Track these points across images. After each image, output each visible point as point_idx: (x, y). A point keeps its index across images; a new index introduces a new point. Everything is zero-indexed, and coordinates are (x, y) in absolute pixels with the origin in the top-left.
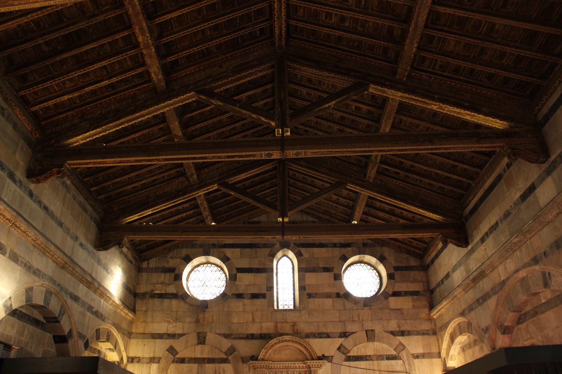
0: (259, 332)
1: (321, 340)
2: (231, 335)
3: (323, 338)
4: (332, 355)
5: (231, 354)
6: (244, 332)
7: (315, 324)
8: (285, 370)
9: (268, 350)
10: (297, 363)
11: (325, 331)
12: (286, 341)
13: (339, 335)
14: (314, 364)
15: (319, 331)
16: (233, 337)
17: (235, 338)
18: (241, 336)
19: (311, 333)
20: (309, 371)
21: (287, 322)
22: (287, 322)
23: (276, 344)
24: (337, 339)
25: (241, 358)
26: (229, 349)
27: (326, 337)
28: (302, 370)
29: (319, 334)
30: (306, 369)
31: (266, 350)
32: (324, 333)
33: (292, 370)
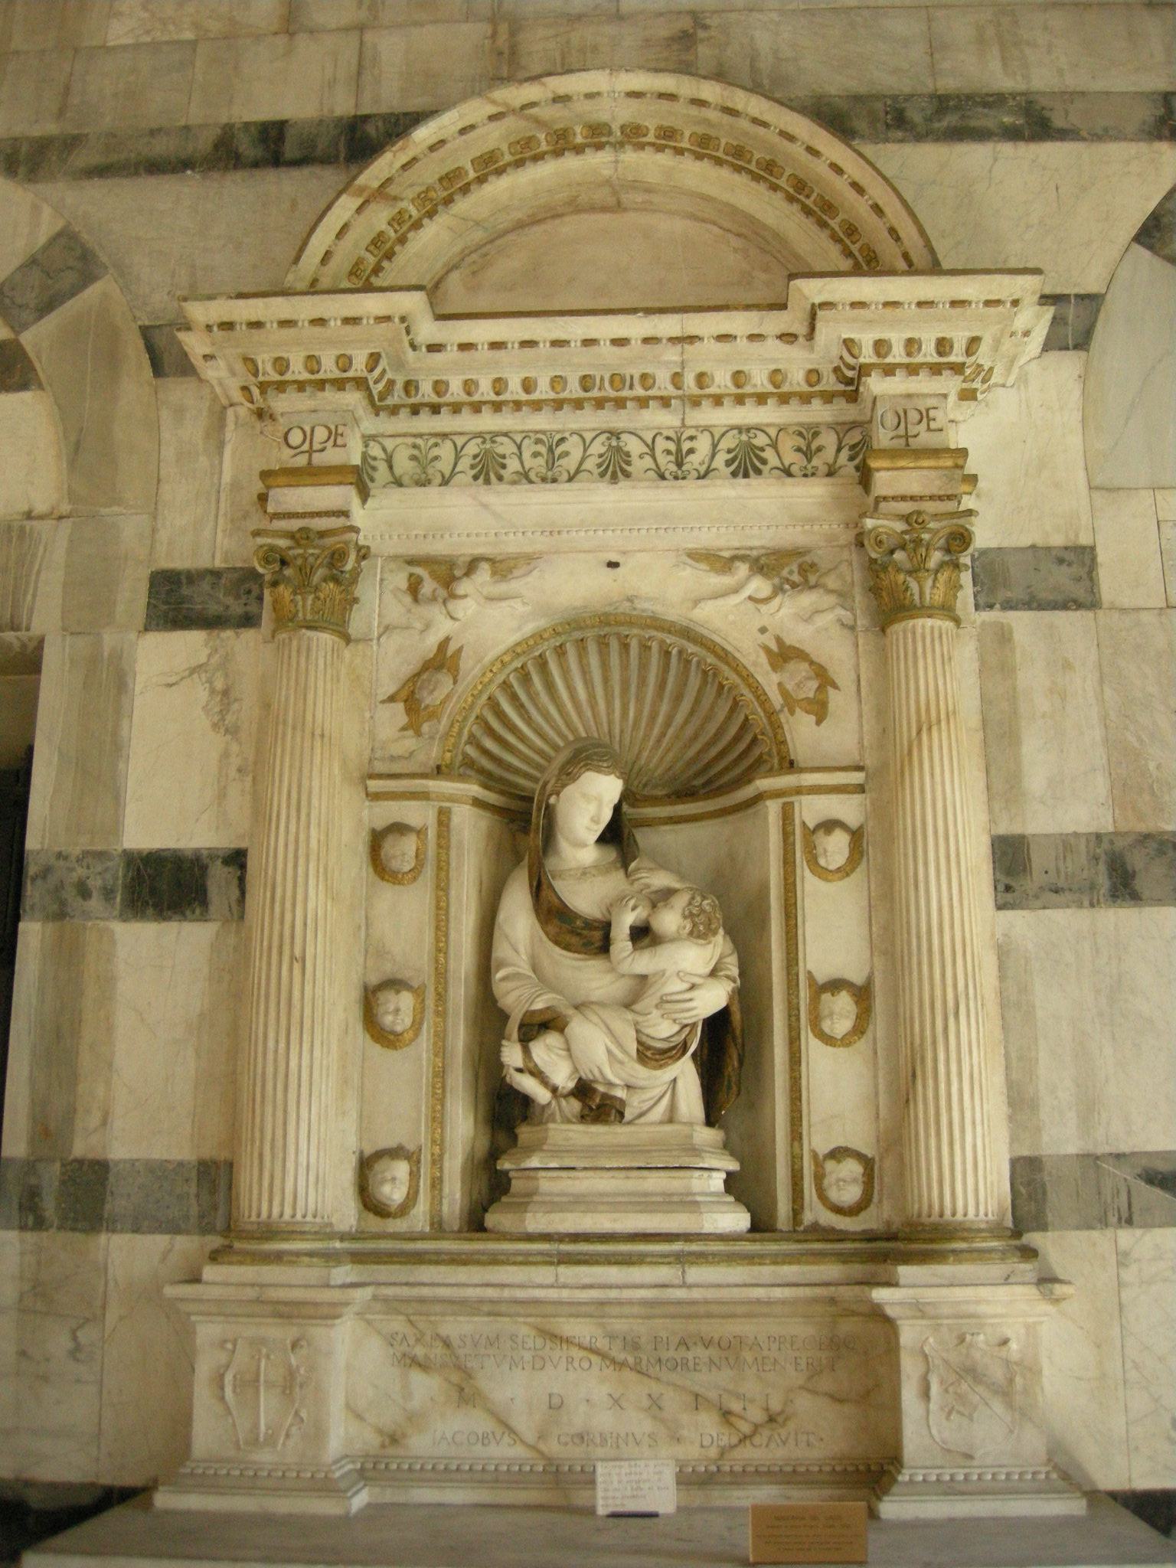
0: (344, 106)
1: (973, 156)
2: (71, 143)
3: (981, 135)
4: (1093, 286)
5: (47, 307)
6: (195, 114)
7: (899, 26)
8: (590, 420)
9: (406, 226)
10: (707, 324)
11: (1005, 83)
12: (598, 136)
13: (1146, 113)
14: (896, 339)
15: (948, 84)
16: (83, 158)
17: (101, 171)
18: (161, 147)
19: (857, 98)
20: (843, 428)
21: (619, 17)
22: (619, 17)
23: (490, 166)
24: (1116, 150)
25: (146, 332)
26: (33, 262)
27: (1013, 134)
28: (769, 415)
29: (942, 103)
30: (819, 412)
31: (380, 218)
32: (996, 100)
33: (657, 418)
